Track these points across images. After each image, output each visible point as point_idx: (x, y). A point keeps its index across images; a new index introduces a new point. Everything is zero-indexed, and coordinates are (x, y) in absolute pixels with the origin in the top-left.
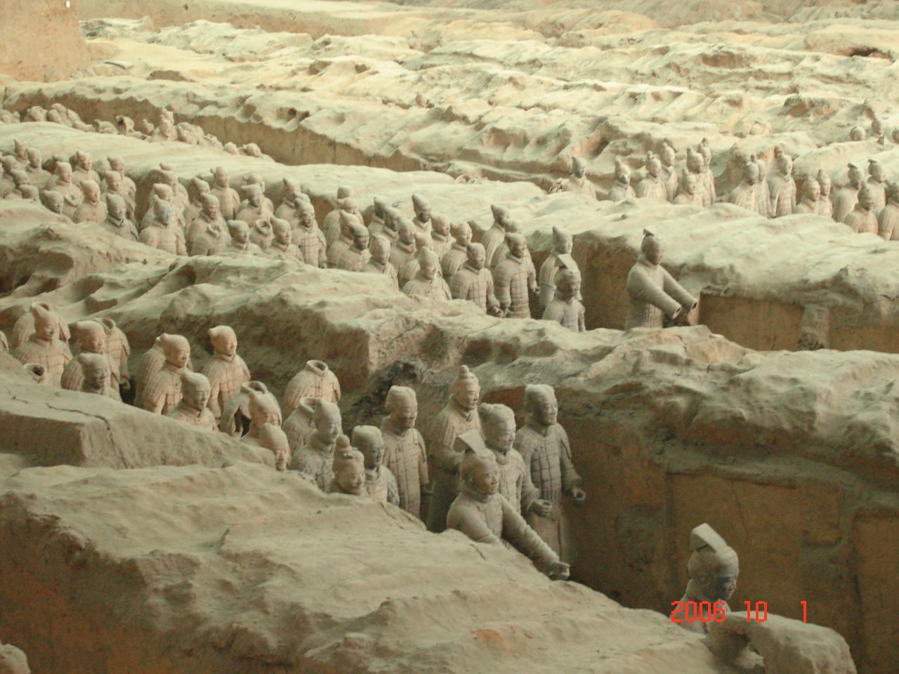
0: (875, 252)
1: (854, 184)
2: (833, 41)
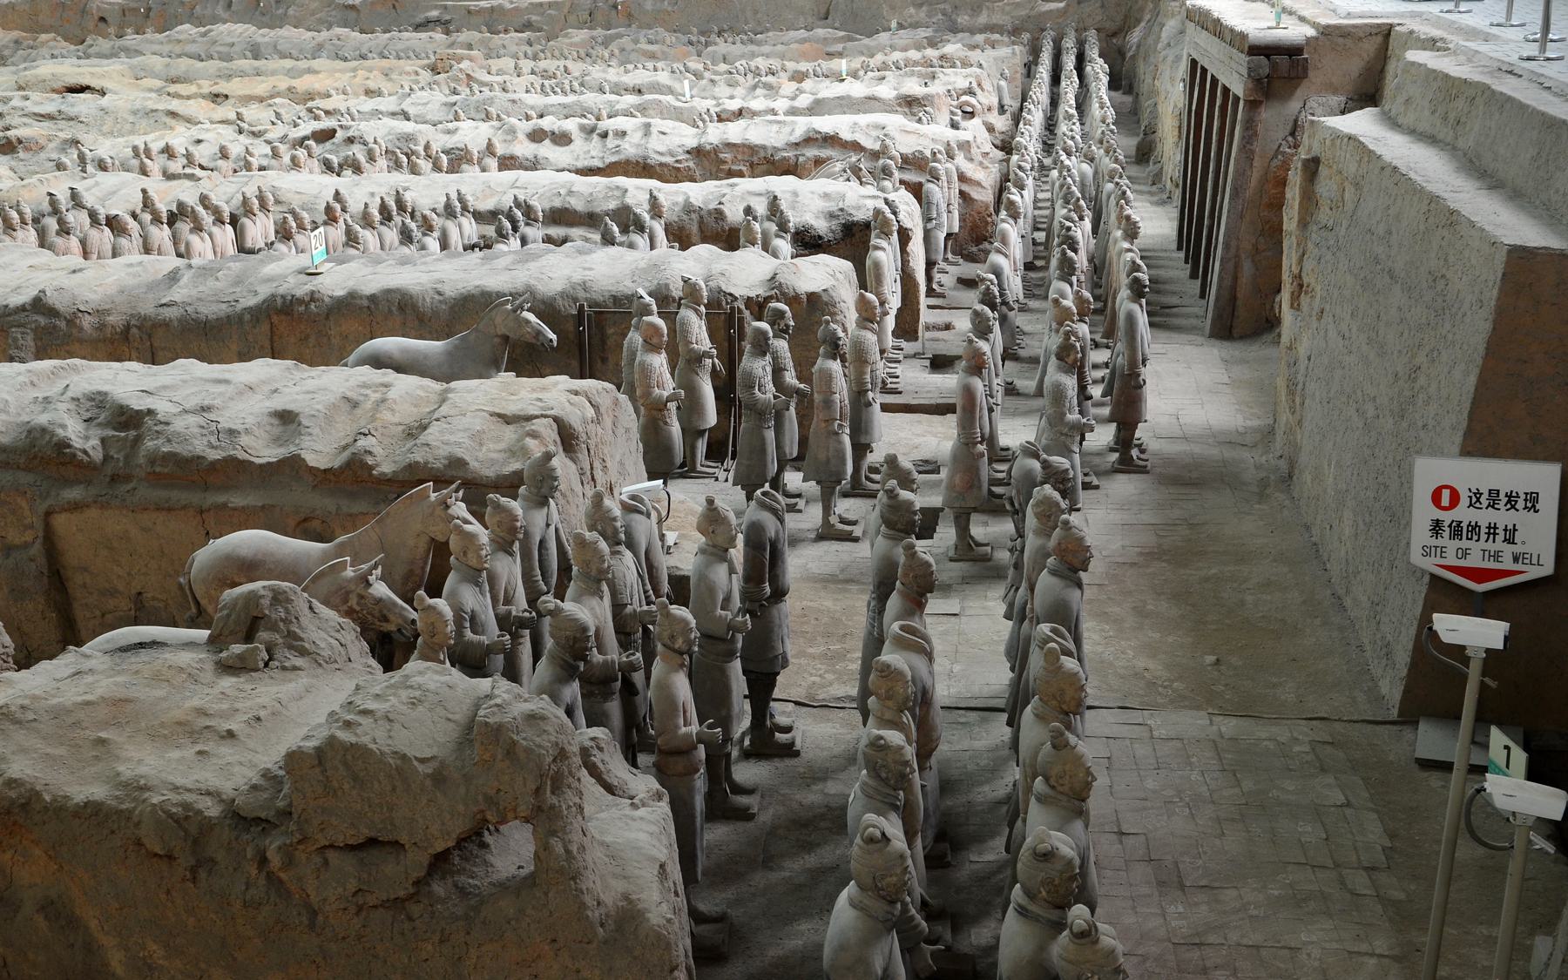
0: (74, 272)
1: (55, 211)
2: (45, 81)
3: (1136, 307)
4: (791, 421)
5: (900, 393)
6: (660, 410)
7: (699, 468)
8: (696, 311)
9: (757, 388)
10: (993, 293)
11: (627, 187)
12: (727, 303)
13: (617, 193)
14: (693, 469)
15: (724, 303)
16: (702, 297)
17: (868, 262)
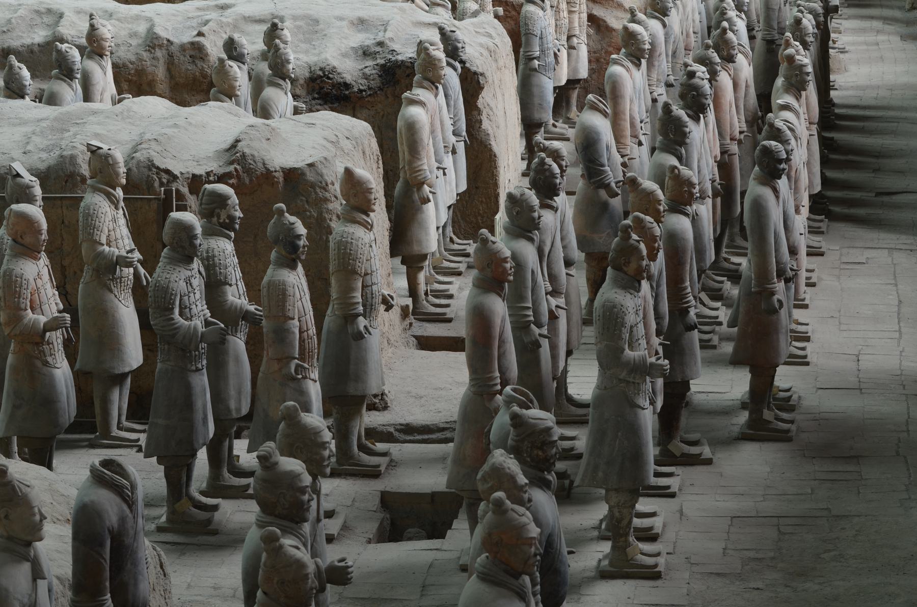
3: (767, 192)
4: (237, 360)
5: (449, 320)
6: (37, 344)
7: (115, 432)
8: (109, 197)
9: (177, 311)
10: (550, 169)
11: (63, 9)
12: (162, 184)
13: (47, 19)
14: (107, 434)
15: (157, 184)
16: (117, 174)
17: (400, 123)
